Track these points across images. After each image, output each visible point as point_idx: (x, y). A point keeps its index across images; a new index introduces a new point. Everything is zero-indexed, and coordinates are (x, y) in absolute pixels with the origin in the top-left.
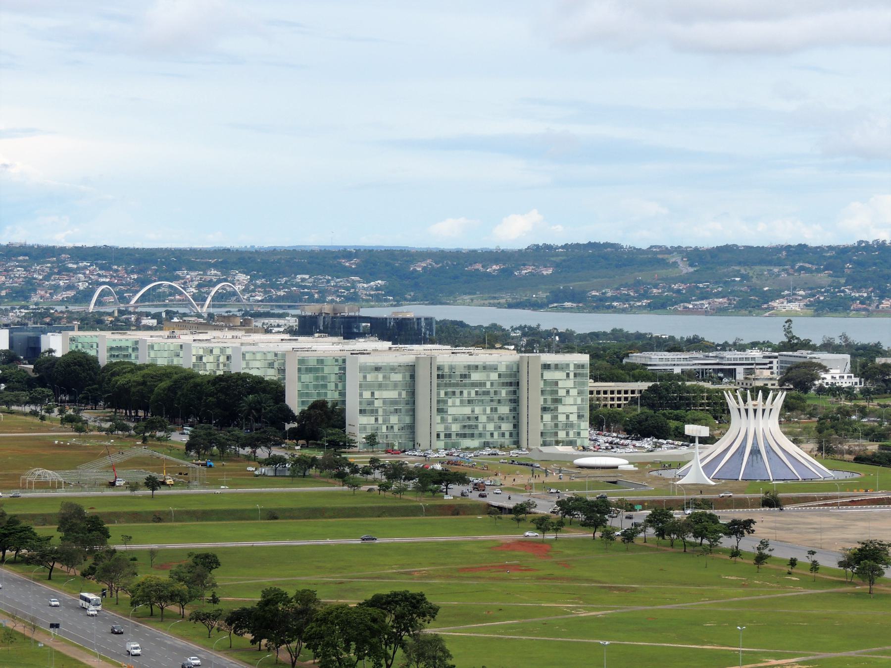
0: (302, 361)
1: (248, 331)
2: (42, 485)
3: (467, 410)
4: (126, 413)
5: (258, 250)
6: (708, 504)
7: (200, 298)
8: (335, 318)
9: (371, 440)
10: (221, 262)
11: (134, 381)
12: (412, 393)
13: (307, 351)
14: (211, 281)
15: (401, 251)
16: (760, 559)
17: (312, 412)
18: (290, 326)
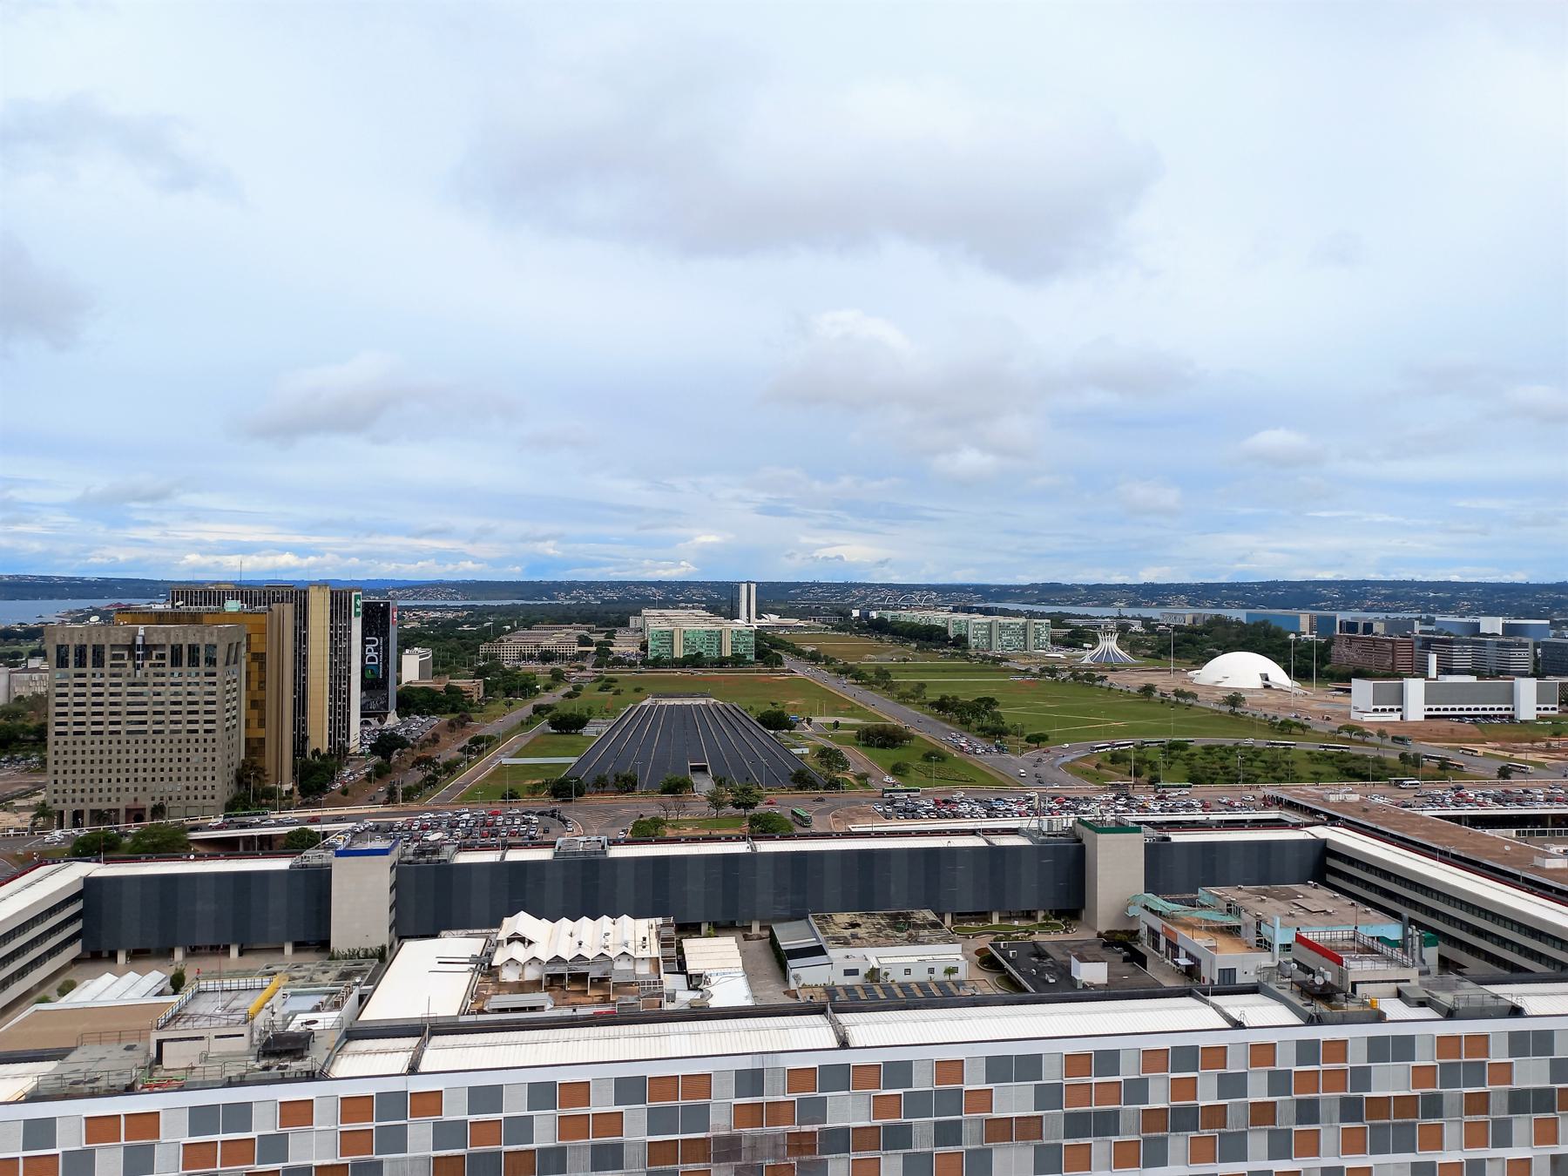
2: (869, 660)
3: (1009, 638)
6: (1092, 670)
7: (920, 600)
9: (977, 647)
12: (990, 632)
16: (1110, 689)
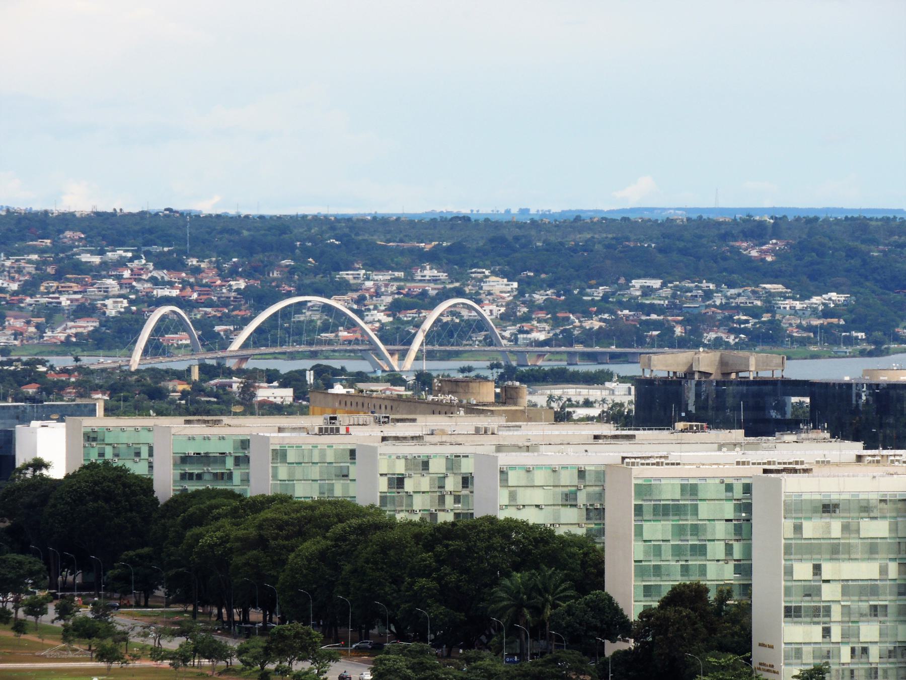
0: (644, 490)
1: (513, 416)
4: (220, 615)
5: (537, 218)
8: (724, 383)
10: (448, 249)
11: (237, 539)
13: (658, 464)
14: (424, 293)
15: (886, 220)
17: (670, 612)
18: (615, 405)
